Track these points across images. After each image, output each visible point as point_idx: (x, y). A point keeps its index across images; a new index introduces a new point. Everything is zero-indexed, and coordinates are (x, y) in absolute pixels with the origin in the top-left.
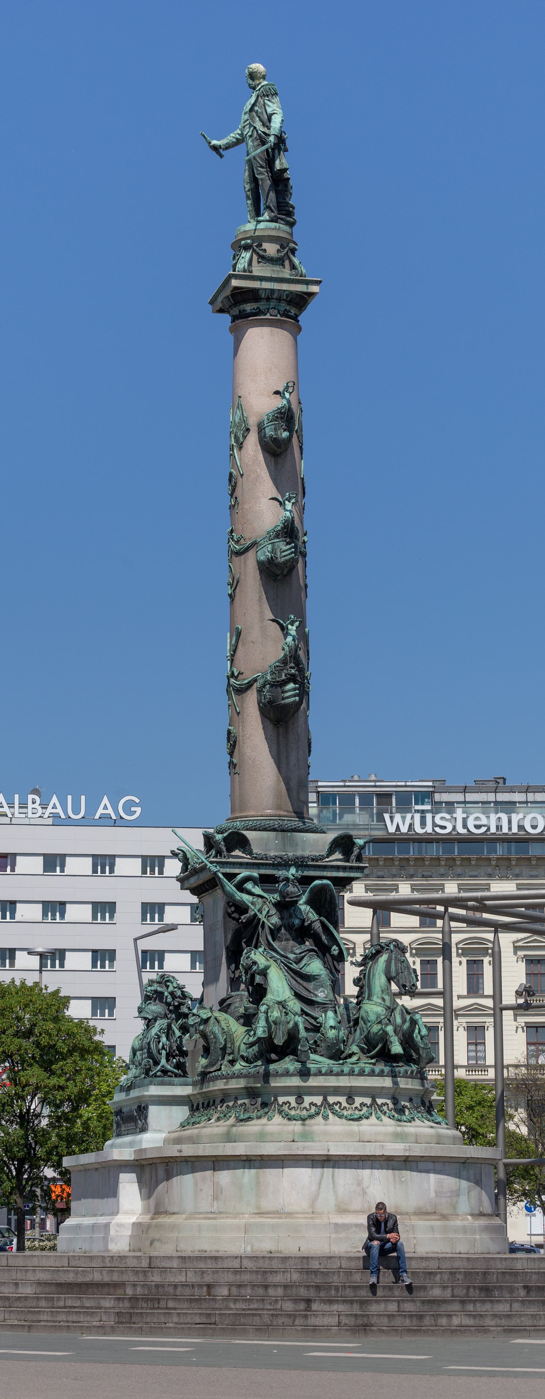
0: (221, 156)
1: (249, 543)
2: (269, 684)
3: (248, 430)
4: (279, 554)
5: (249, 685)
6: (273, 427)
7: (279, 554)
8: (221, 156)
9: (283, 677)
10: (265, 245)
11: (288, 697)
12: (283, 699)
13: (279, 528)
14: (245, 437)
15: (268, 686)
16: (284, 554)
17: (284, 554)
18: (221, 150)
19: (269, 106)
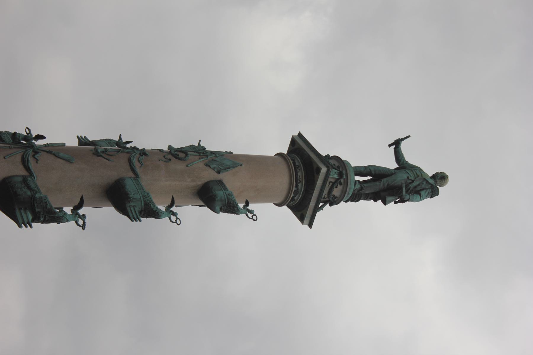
0: (390, 146)
1: (138, 170)
2: (32, 196)
3: (219, 172)
4: (132, 204)
5: (28, 169)
6: (223, 198)
7: (132, 204)
8: (390, 146)
9: (37, 210)
10: (340, 187)
11: (21, 214)
12: (20, 209)
13: (152, 206)
14: (214, 169)
15: (29, 193)
16: (132, 209)
17: (132, 209)
18: (394, 146)
19: (426, 192)
